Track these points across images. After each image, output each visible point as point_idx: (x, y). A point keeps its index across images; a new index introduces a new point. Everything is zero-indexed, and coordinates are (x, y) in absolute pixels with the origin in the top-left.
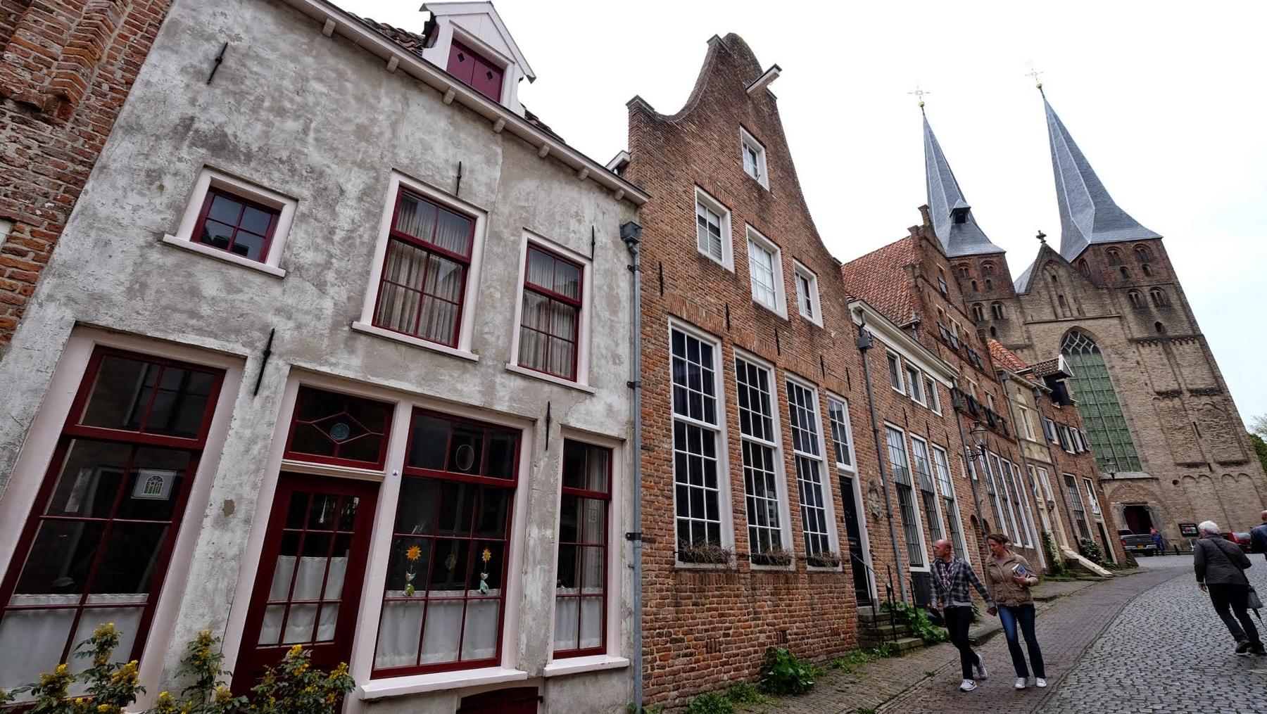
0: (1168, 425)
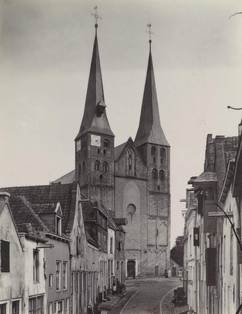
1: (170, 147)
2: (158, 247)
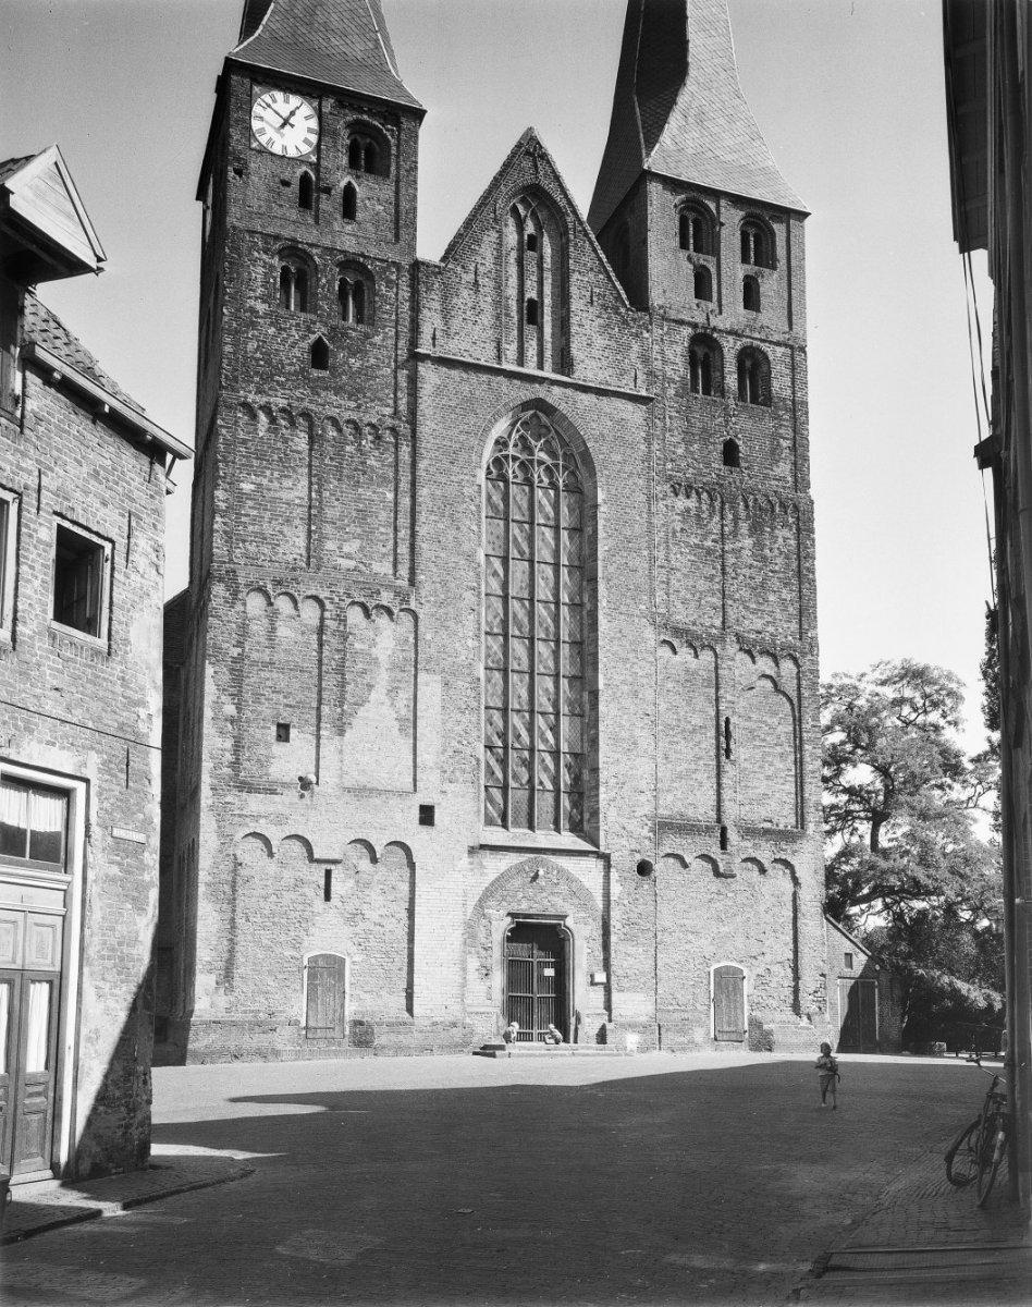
0: (670, 718)
1: (802, 215)
2: (732, 835)
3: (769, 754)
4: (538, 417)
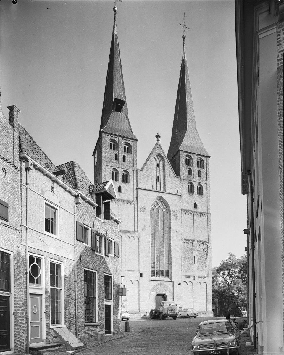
1: (209, 157)
3: (202, 263)
4: (160, 198)
